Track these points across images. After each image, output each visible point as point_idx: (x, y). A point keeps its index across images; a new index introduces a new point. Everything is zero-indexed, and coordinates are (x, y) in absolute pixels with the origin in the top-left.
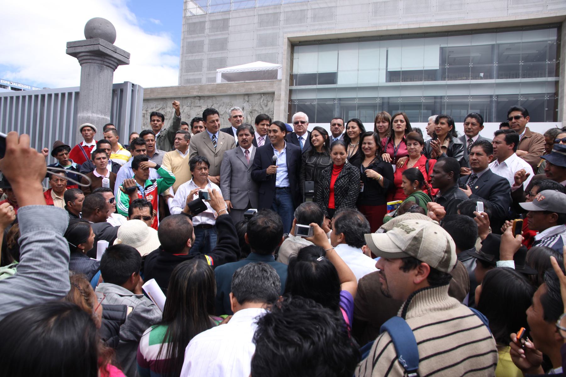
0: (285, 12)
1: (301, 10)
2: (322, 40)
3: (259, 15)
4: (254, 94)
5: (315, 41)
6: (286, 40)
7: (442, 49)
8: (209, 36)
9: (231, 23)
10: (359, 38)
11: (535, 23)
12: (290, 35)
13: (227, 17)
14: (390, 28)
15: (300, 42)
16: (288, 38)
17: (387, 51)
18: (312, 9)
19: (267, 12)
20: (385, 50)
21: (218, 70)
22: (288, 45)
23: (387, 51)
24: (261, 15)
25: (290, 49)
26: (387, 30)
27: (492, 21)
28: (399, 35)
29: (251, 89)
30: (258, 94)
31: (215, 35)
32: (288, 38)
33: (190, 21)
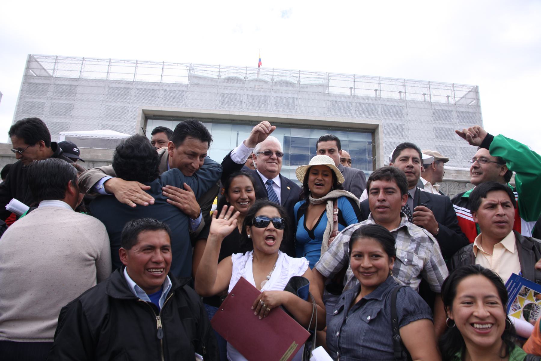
0: (136, 88)
1: (153, 90)
2: (177, 117)
3: (109, 87)
4: (101, 162)
5: (169, 116)
6: (141, 111)
7: (285, 138)
8: (51, 99)
9: (79, 90)
10: (213, 119)
11: (357, 127)
12: (145, 108)
13: (75, 83)
14: (242, 114)
15: (154, 116)
16: (143, 110)
17: (238, 134)
18: (163, 90)
19: (117, 85)
20: (236, 133)
21: (61, 133)
22: (142, 117)
23: (238, 134)
24: (111, 87)
25: (143, 121)
26: (239, 115)
27: (326, 120)
28: (250, 121)
29: (97, 156)
30: (105, 162)
31: (59, 99)
32: (143, 110)
33: (32, 81)
